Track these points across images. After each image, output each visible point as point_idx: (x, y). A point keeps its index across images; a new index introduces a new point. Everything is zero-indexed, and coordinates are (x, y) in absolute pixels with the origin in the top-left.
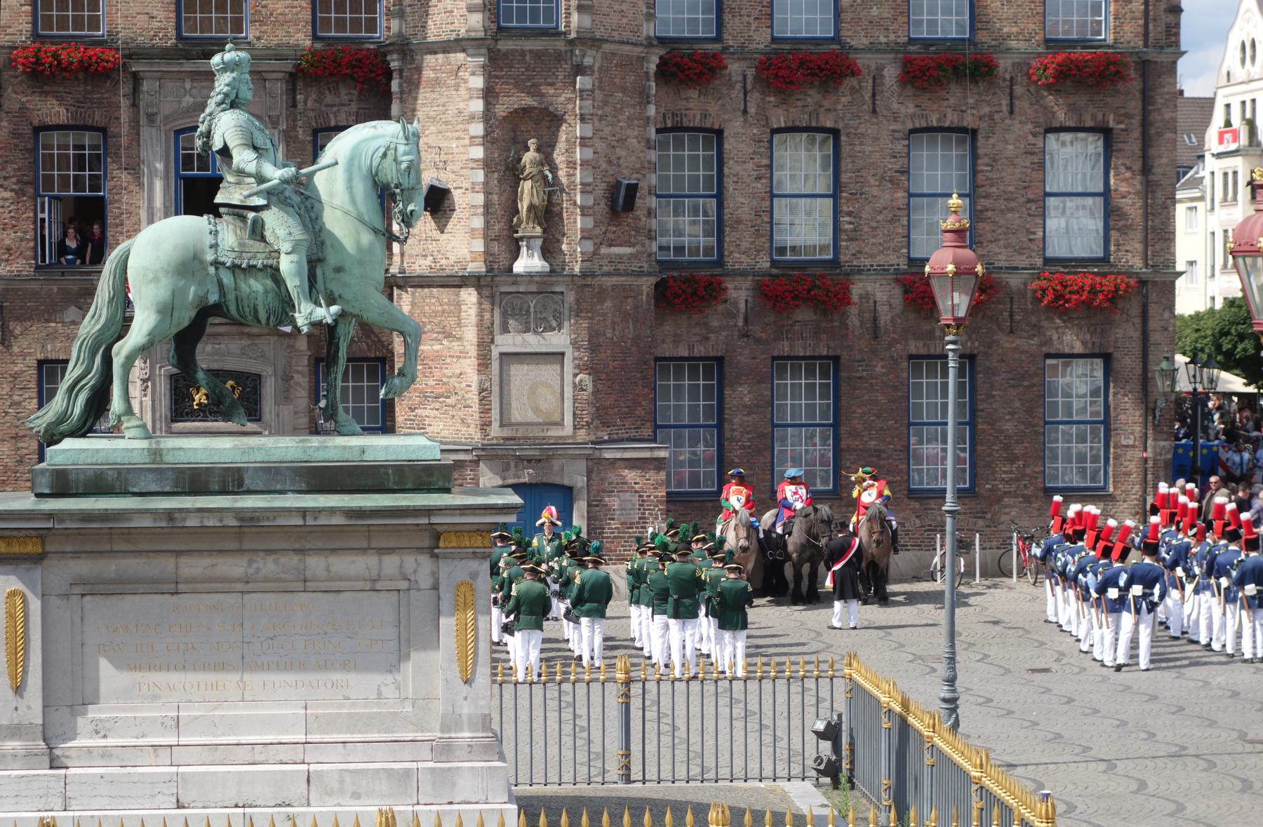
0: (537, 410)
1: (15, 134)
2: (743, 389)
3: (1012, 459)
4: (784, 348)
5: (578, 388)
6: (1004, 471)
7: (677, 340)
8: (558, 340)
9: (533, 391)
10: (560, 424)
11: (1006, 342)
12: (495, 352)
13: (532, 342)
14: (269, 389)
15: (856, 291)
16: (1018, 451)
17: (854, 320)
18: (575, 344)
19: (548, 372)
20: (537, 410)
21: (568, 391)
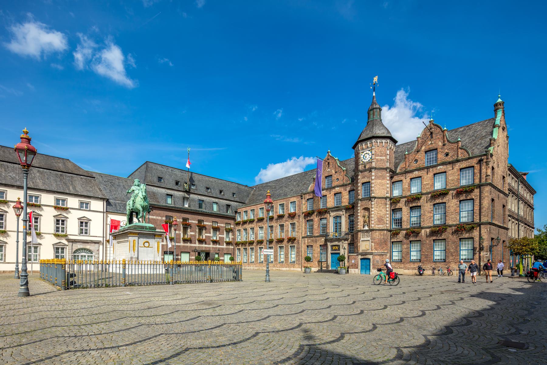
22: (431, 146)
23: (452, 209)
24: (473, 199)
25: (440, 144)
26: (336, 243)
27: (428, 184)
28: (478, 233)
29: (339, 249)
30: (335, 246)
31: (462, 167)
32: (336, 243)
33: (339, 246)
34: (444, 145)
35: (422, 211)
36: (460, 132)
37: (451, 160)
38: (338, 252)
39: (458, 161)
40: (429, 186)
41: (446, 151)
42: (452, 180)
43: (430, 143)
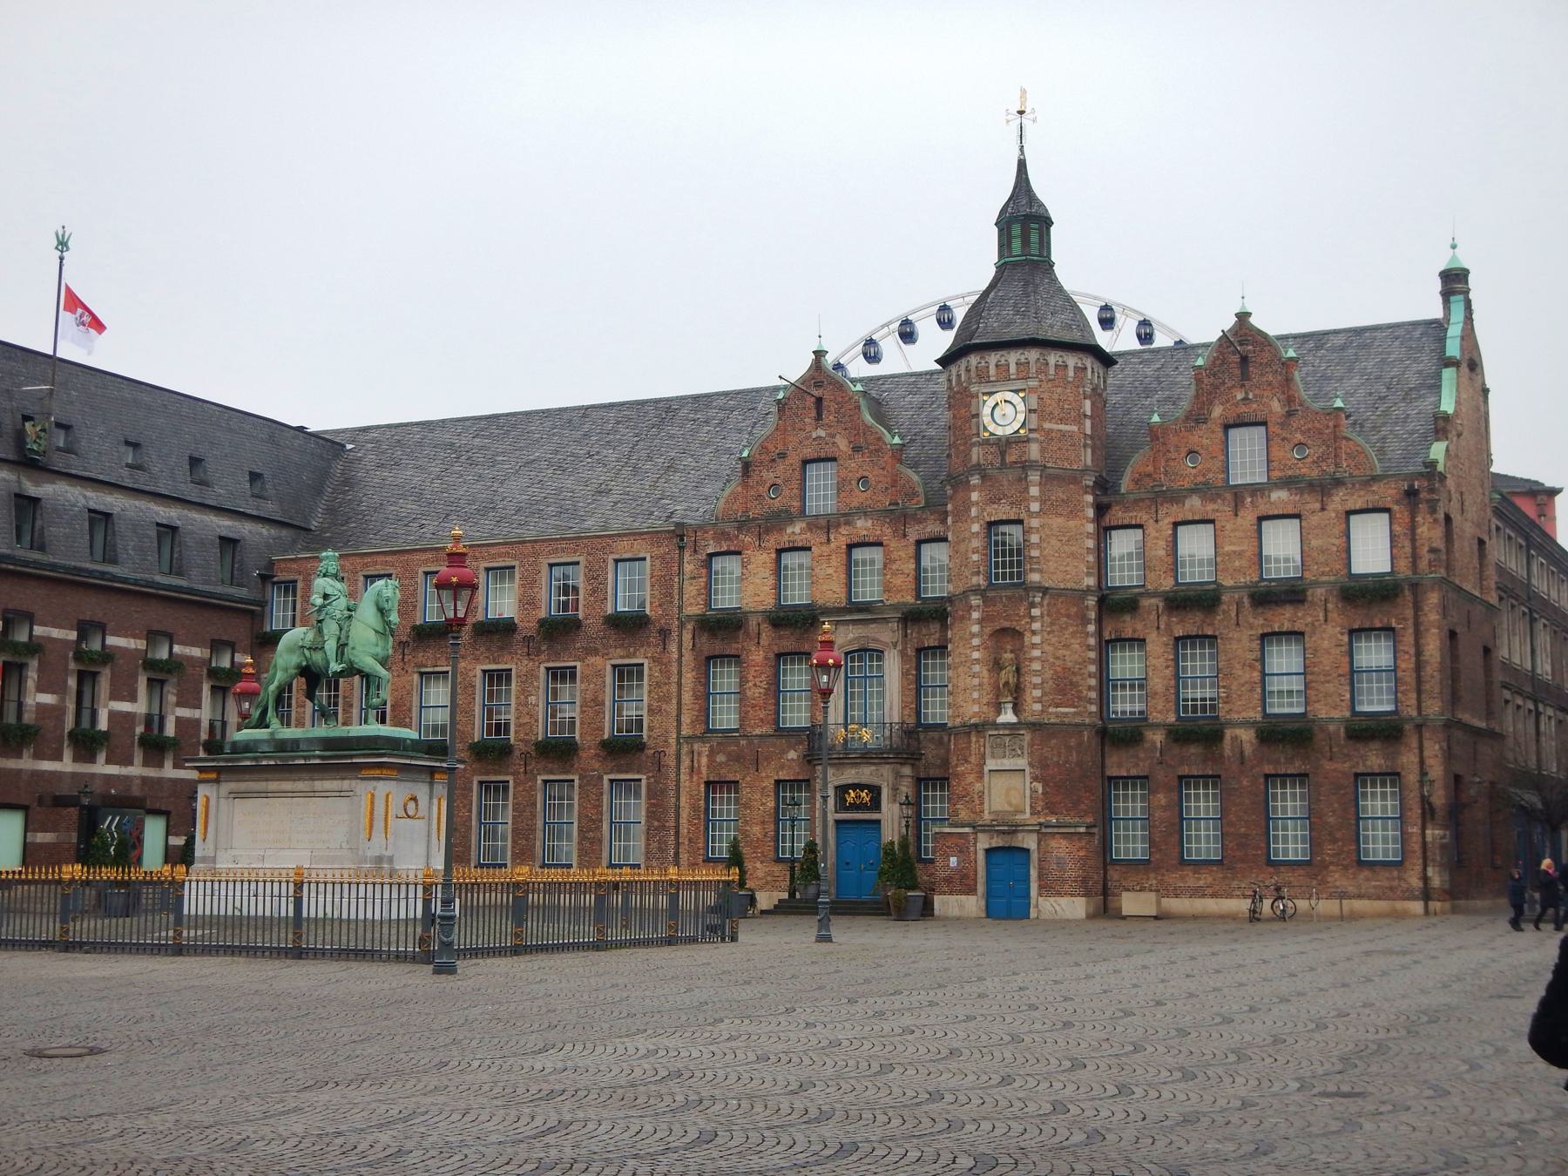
0: (1010, 804)
1: (766, 658)
2: (1161, 796)
3: (1334, 841)
4: (1185, 770)
5: (1034, 791)
6: (1329, 849)
7: (1120, 766)
8: (1022, 763)
9: (1008, 790)
10: (1023, 812)
11: (1328, 765)
12: (986, 769)
13: (1007, 763)
14: (885, 794)
15: (1228, 733)
16: (1338, 835)
17: (1227, 752)
18: (1030, 764)
19: (1016, 781)
20: (1010, 804)
21: (1028, 792)
22: (1243, 409)
23: (1326, 662)
24: (1393, 629)
25: (1276, 406)
26: (866, 774)
27: (1240, 554)
28: (1417, 760)
29: (876, 805)
30: (855, 786)
31: (1351, 506)
32: (866, 774)
33: (875, 791)
34: (1290, 414)
35: (1222, 657)
36: (1333, 349)
37: (1315, 473)
38: (874, 816)
39: (1338, 483)
40: (1244, 563)
41: (1299, 437)
42: (1323, 551)
43: (1240, 396)
